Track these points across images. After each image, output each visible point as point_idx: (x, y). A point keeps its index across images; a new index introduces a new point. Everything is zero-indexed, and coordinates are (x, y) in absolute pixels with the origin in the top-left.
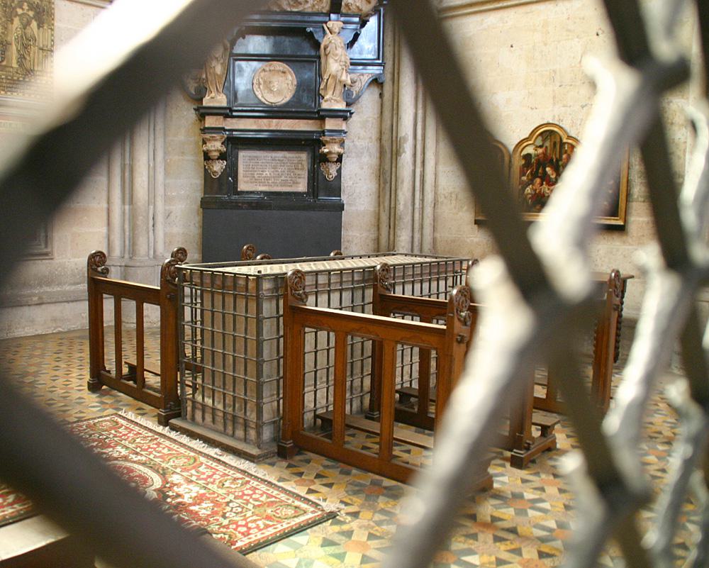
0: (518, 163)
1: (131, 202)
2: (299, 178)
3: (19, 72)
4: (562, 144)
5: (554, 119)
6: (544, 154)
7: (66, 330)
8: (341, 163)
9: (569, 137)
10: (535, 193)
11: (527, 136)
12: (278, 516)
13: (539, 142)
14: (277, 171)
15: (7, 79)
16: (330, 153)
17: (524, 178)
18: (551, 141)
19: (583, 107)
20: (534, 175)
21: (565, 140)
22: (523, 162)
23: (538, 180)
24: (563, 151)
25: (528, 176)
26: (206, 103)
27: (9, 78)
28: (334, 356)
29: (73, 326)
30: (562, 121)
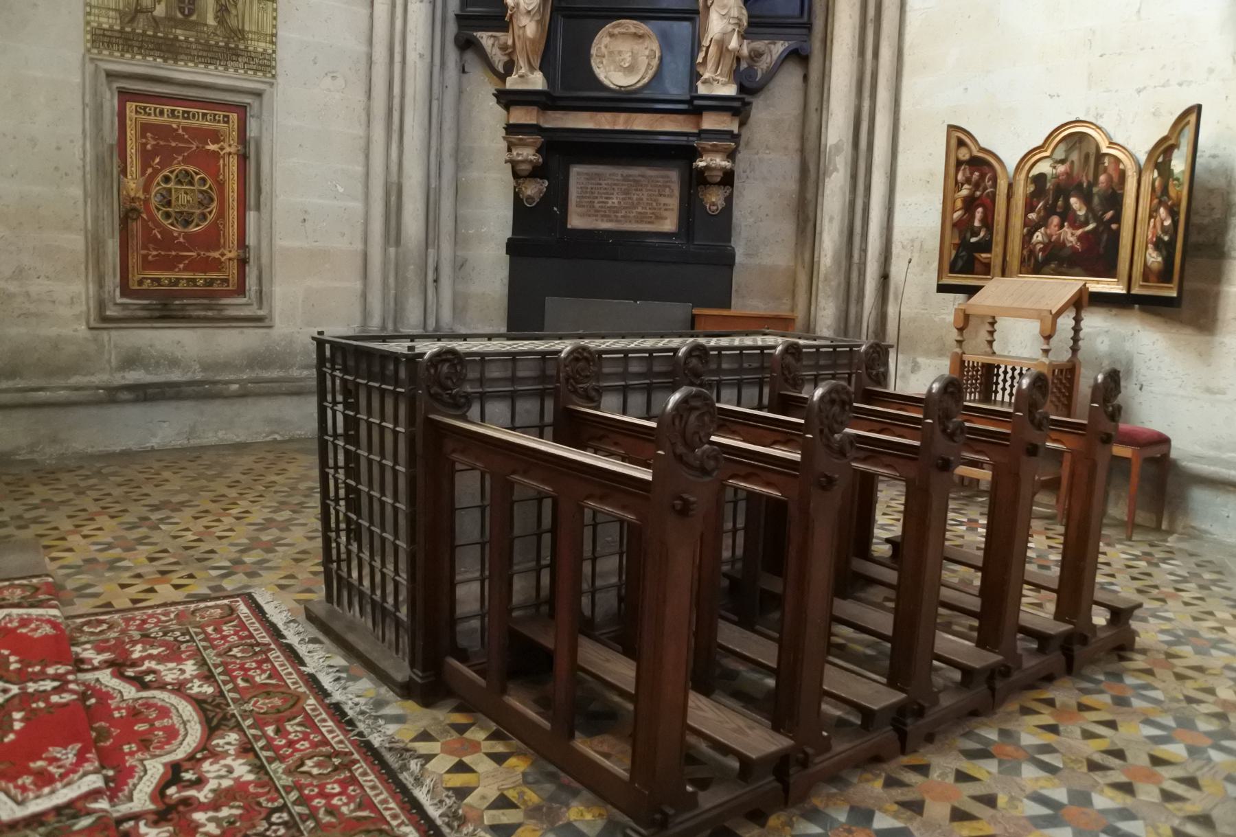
0: (1022, 190)
1: (398, 242)
2: (666, 210)
3: (218, 32)
4: (1100, 156)
5: (1087, 113)
6: (1069, 174)
7: (287, 438)
8: (732, 186)
9: (1112, 144)
10: (1050, 241)
11: (1040, 143)
12: (262, 711)
13: (1059, 154)
14: (629, 198)
15: (197, 42)
16: (707, 168)
17: (1032, 216)
18: (1080, 152)
19: (1139, 91)
20: (1050, 211)
21: (1104, 150)
22: (1031, 188)
23: (1055, 220)
24: (1101, 167)
25: (1039, 213)
26: (511, 84)
27: (202, 41)
28: (378, 446)
29: (299, 432)
30: (1101, 116)
